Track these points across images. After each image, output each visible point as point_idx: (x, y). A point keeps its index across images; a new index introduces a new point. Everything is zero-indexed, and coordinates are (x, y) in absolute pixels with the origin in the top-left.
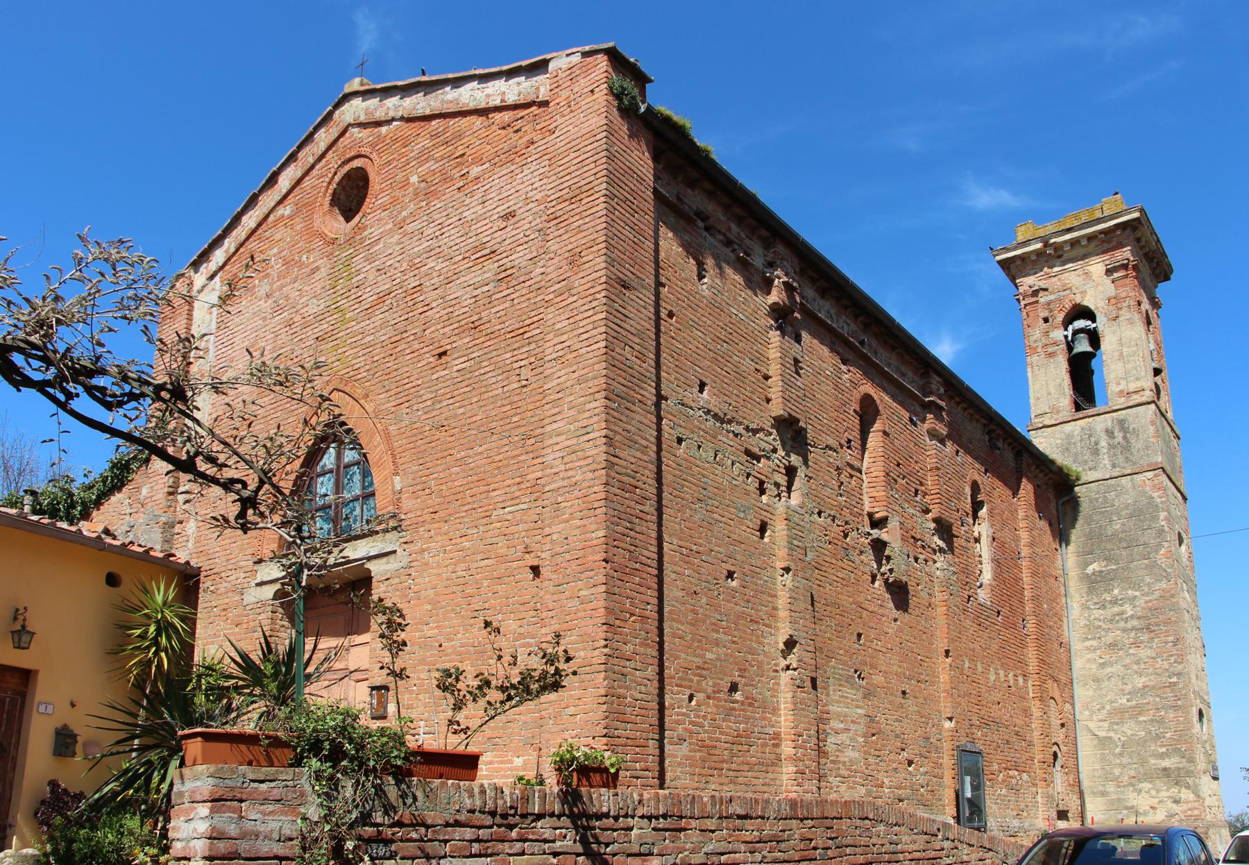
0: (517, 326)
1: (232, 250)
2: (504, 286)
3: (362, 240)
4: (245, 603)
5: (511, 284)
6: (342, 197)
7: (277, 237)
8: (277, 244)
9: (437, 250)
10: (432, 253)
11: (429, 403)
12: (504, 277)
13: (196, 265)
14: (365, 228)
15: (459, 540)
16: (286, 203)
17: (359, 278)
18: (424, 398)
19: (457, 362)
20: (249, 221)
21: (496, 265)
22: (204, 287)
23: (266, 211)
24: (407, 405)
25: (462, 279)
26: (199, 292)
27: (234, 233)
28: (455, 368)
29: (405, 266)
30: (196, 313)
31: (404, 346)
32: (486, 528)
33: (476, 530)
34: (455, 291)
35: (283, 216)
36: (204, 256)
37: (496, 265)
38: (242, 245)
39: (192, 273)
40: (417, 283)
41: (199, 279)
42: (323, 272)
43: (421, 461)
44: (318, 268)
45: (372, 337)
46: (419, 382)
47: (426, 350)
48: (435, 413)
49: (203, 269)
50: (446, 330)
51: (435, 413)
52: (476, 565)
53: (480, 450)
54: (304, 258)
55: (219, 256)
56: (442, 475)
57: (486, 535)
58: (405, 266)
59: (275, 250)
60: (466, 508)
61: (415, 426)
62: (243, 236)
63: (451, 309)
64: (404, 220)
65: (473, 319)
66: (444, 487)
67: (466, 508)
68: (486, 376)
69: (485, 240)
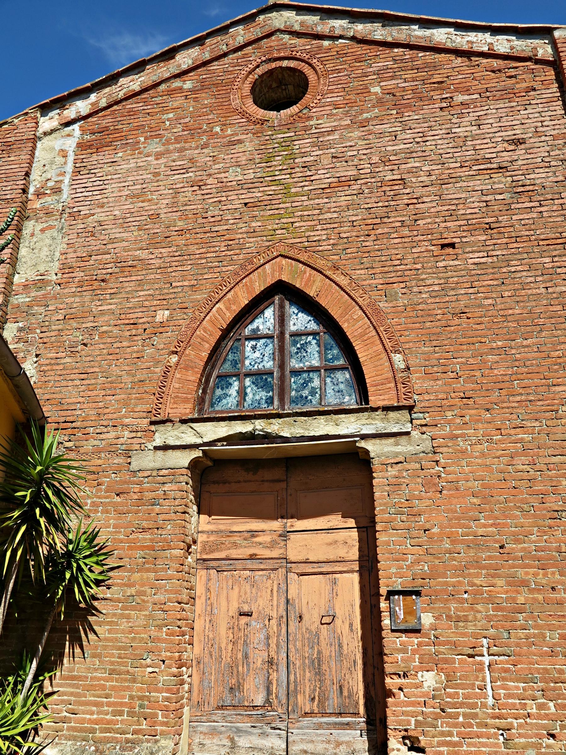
0: (554, 236)
1: (103, 103)
2: (524, 198)
3: (306, 129)
4: (135, 466)
5: (534, 199)
6: (257, 90)
7: (176, 104)
8: (173, 111)
9: (420, 154)
10: (414, 155)
11: (436, 288)
12: (520, 191)
13: (45, 109)
14: (309, 118)
15: (513, 432)
16: (185, 78)
17: (305, 159)
18: (428, 282)
19: (471, 255)
20: (132, 83)
21: (509, 179)
22: (53, 131)
23: (155, 78)
24: (403, 285)
25: (465, 184)
26: (45, 134)
27: (107, 90)
28: (470, 261)
29: (375, 159)
30: (37, 153)
31: (386, 230)
32: (549, 423)
33: (537, 424)
34: (451, 192)
35: (181, 88)
36: (60, 103)
37: (509, 179)
38: (117, 103)
39: (39, 115)
40: (399, 177)
41: (47, 123)
42: (249, 146)
43: (435, 343)
44: (240, 142)
45: (335, 215)
46: (419, 266)
47: (422, 238)
48: (447, 299)
49: (54, 113)
50: (449, 224)
51: (447, 299)
52: (548, 460)
53: (525, 343)
54: (218, 129)
55: (81, 106)
56: (471, 361)
57: (554, 430)
58: (375, 159)
59: (171, 115)
60: (518, 398)
61: (421, 307)
62: (121, 95)
63: (454, 207)
64: (368, 120)
65: (487, 220)
66: (478, 374)
67: (518, 398)
68: (519, 275)
69: (488, 156)
